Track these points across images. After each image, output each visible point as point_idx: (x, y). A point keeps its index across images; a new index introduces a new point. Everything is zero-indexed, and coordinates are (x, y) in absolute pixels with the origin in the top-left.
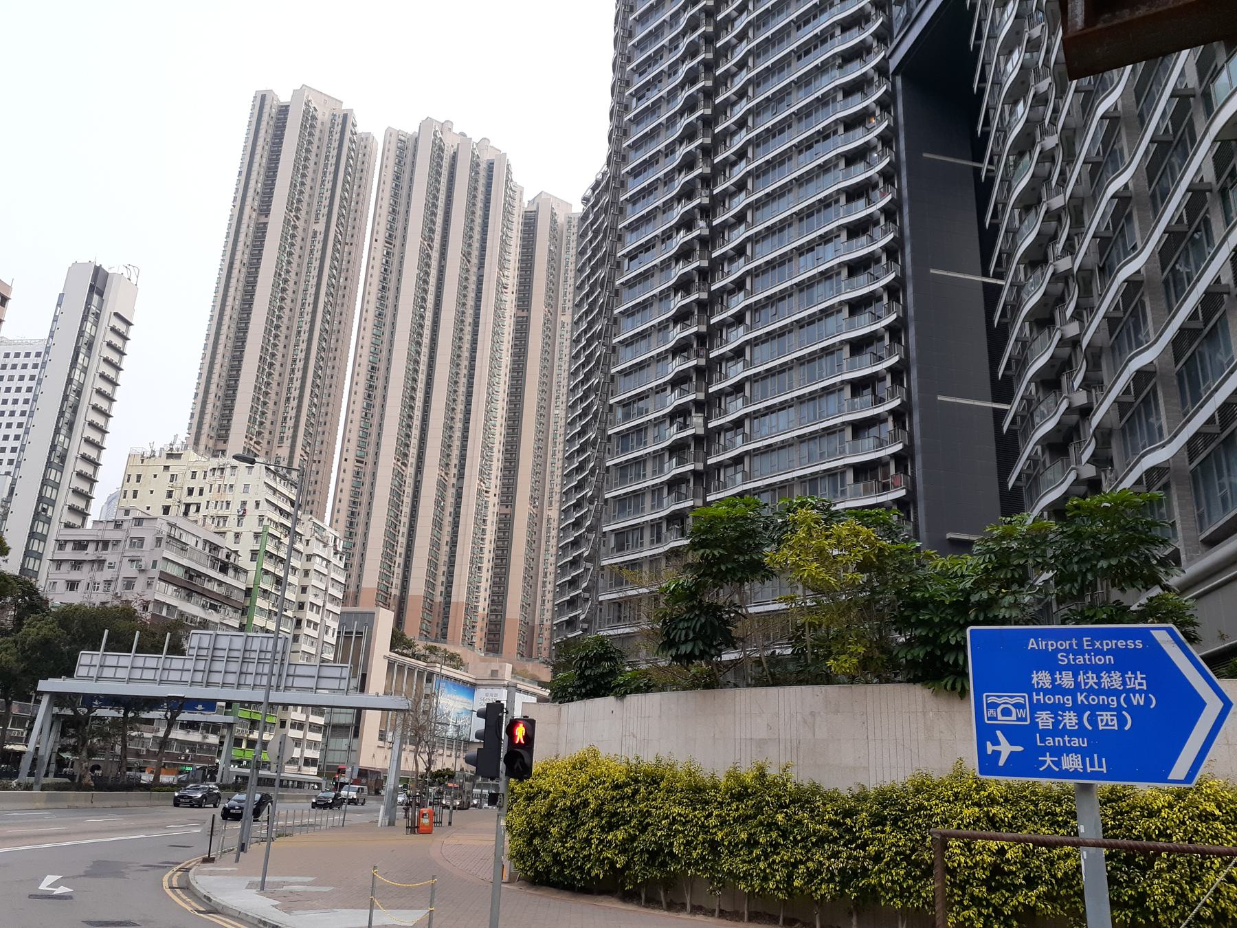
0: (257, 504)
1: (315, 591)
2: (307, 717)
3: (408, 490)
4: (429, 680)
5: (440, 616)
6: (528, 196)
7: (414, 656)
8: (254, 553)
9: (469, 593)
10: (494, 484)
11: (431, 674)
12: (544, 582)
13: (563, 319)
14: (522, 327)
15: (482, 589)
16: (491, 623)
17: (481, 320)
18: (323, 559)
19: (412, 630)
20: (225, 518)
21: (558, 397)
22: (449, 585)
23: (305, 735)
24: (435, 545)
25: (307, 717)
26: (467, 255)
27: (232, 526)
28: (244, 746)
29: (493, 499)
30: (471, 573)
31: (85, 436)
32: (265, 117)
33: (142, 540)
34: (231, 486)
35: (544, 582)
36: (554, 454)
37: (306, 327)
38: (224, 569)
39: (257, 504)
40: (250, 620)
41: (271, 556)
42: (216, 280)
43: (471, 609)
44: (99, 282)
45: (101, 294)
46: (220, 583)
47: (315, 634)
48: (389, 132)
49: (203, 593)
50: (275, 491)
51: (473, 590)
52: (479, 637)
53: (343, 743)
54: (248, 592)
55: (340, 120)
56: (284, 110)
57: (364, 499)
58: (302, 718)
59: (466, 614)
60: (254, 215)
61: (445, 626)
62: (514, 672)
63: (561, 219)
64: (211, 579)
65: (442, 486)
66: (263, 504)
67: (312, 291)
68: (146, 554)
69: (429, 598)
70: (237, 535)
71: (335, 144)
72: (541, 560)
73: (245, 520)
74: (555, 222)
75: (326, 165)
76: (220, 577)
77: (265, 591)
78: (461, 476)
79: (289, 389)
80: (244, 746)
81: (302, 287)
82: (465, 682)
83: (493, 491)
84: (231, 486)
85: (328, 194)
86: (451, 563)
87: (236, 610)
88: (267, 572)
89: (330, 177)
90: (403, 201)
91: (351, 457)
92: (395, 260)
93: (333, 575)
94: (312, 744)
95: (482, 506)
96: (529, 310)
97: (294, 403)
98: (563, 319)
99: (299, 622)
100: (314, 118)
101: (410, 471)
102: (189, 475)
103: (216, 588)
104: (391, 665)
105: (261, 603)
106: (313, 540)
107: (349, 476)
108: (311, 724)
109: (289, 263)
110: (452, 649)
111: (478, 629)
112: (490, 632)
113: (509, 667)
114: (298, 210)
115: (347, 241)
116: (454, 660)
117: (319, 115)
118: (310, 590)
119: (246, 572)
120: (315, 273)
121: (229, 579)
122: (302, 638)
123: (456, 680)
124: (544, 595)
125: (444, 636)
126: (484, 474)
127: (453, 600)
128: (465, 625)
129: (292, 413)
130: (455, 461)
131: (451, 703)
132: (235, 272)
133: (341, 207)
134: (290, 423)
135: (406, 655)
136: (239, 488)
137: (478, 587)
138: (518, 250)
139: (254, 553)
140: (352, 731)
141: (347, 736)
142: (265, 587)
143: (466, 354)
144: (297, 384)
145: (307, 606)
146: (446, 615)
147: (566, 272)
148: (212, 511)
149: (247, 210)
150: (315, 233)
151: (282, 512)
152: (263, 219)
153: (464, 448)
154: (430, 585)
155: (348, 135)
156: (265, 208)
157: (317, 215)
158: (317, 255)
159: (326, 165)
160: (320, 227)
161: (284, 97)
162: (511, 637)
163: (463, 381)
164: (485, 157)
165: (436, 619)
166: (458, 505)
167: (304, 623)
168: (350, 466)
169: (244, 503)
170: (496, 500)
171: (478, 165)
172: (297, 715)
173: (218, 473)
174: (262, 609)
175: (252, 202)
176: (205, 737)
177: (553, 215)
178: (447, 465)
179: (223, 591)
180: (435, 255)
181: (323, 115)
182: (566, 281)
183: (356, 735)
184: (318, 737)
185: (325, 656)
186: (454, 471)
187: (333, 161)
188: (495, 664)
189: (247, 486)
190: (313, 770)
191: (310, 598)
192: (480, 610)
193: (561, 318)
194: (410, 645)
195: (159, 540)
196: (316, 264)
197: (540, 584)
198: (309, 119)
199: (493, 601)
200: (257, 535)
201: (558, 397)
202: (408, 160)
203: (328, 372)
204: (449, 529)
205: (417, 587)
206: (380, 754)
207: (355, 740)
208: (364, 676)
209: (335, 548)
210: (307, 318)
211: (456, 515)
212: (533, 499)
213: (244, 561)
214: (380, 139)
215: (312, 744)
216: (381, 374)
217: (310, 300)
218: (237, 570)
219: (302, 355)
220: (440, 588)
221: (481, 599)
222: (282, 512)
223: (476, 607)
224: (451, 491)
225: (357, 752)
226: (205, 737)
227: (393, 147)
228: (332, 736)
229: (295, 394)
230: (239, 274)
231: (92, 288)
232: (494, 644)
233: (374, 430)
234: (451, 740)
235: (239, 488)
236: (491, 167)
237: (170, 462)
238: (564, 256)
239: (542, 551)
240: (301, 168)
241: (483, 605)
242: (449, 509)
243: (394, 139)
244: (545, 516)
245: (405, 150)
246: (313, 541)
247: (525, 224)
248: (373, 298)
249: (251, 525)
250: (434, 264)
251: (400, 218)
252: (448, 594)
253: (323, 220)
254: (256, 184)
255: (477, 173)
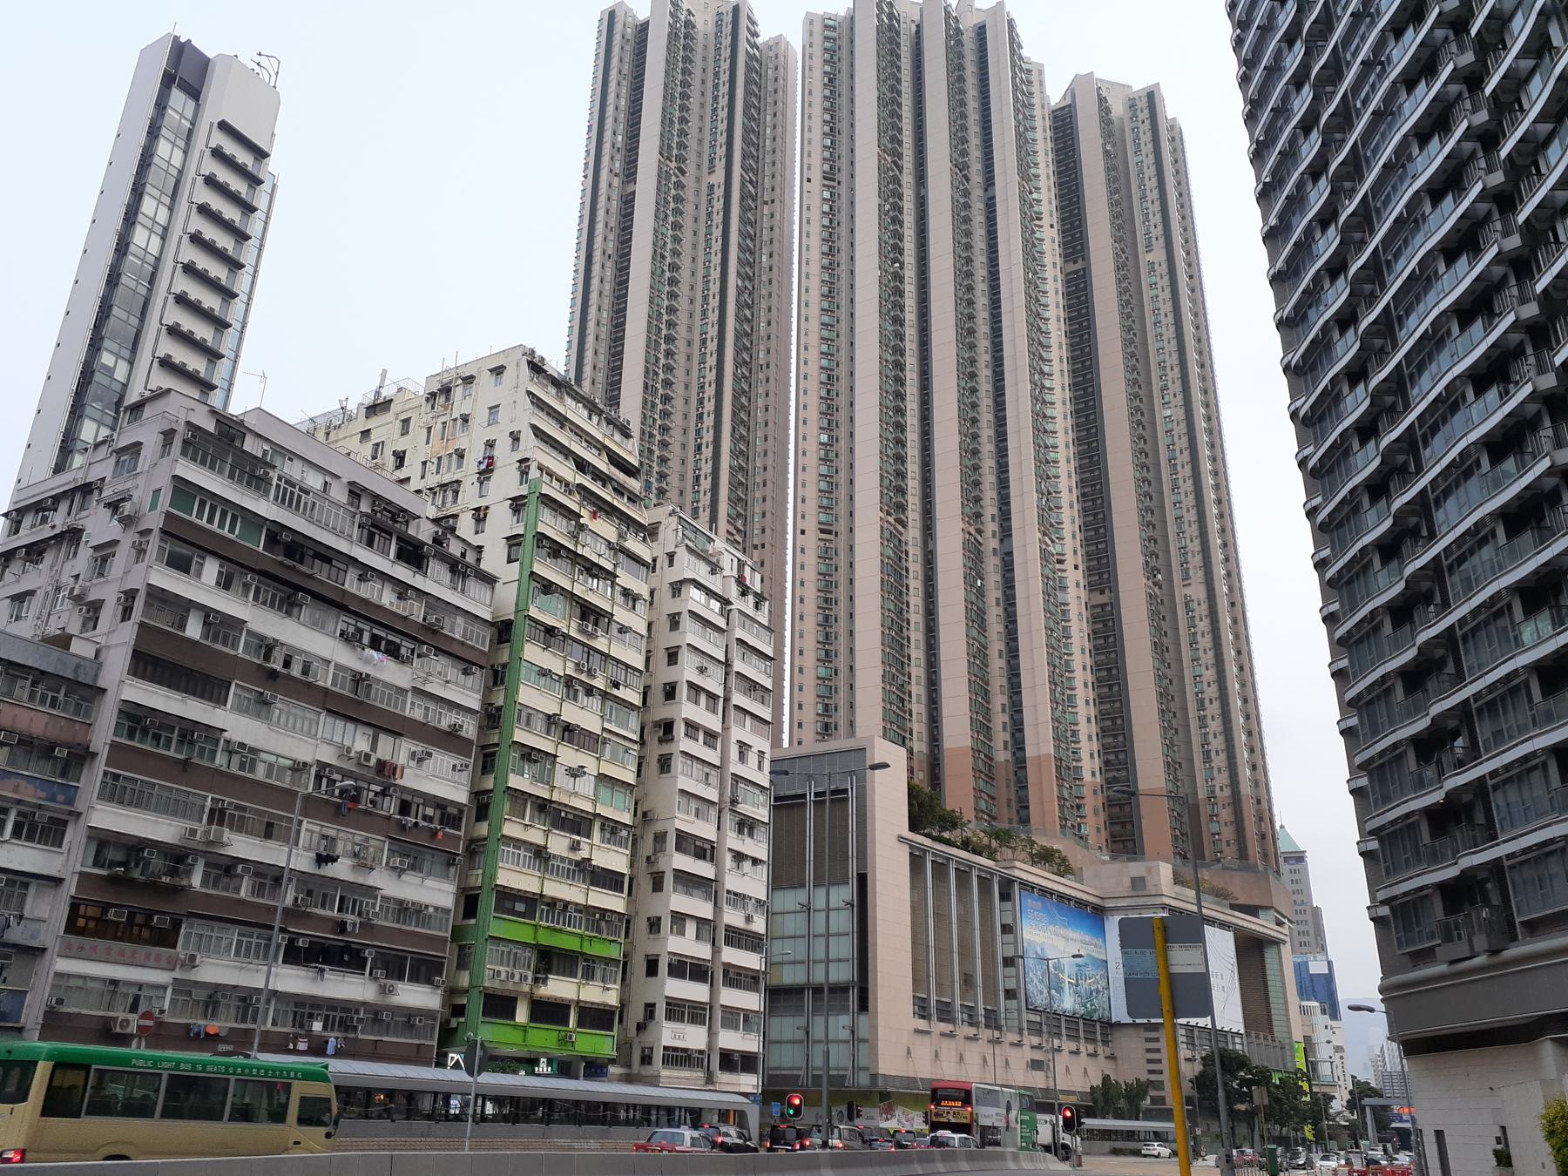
0: (515, 437)
1: (696, 660)
2: (716, 951)
3: (915, 566)
4: (1006, 896)
5: (1007, 780)
6: (1055, 93)
7: (965, 845)
8: (514, 541)
9: (1057, 738)
10: (1071, 544)
11: (1007, 885)
12: (1202, 719)
13: (1150, 257)
14: (1078, 291)
15: (1083, 737)
16: (1110, 803)
17: (1010, 412)
18: (710, 593)
19: (959, 794)
20: (454, 487)
21: (1164, 388)
22: (1017, 727)
23: (713, 993)
24: (978, 656)
25: (716, 951)
26: (960, 168)
27: (469, 497)
28: (522, 1015)
29: (1074, 576)
30: (1054, 701)
31: (161, 353)
32: (617, 39)
33: (136, 447)
34: (465, 419)
35: (1202, 719)
36: (1175, 488)
37: (713, 332)
38: (413, 554)
39: (515, 437)
40: (512, 694)
41: (556, 551)
42: (570, 289)
43: (1066, 771)
44: (184, 71)
45: (195, 93)
46: (403, 589)
47: (713, 756)
48: (810, 20)
49: (338, 604)
50: (562, 421)
51: (1065, 736)
52: (1093, 823)
53: (840, 1025)
54: (503, 631)
55: (730, 18)
56: (643, 29)
57: (841, 593)
58: (703, 951)
59: (1060, 778)
60: (616, 182)
61: (1024, 805)
62: (1178, 880)
63: (1118, 109)
64: (366, 572)
65: (974, 552)
66: (528, 439)
67: (715, 274)
68: (141, 480)
69: (985, 767)
70: (480, 515)
71: (726, 53)
72: (1188, 680)
73: (495, 476)
74: (1108, 111)
75: (716, 86)
76: (402, 572)
77: (550, 631)
78: (1006, 533)
79: (698, 432)
80: (522, 1015)
81: (701, 272)
82: (1081, 904)
83: (1070, 560)
84: (465, 419)
85: (723, 126)
86: (1014, 688)
87: (466, 662)
88: (548, 587)
89: (723, 101)
90: (844, 113)
91: (811, 525)
92: (843, 202)
93: (739, 633)
94: (733, 1017)
95: (1053, 587)
96: (1085, 258)
97: (707, 452)
98: (1150, 257)
99: (668, 727)
100: (689, 24)
101: (913, 533)
102: (398, 425)
103: (388, 598)
104: (916, 861)
105: (533, 653)
106: (682, 554)
107: (811, 559)
108: (728, 968)
109: (677, 240)
110: (1042, 841)
111: (1088, 810)
112: (1112, 821)
113: (1165, 871)
114: (681, 159)
115: (756, 195)
116: (1045, 857)
117: (700, 26)
118: (685, 656)
119: (489, 580)
120: (717, 246)
121: (435, 581)
122: (678, 763)
123: (1062, 897)
124: (1205, 743)
125: (1025, 821)
126: (1048, 527)
127: (1030, 752)
128: (1061, 798)
129: (707, 468)
130: (990, 509)
131: (1060, 943)
132: (596, 268)
133: (745, 140)
134: (706, 484)
135: (948, 842)
136: (480, 417)
137: (1074, 733)
138: (1050, 145)
139: (514, 541)
140: (853, 996)
141: (844, 1009)
142: (550, 621)
143: (983, 328)
144: (709, 421)
145: (683, 692)
146: (1022, 785)
147: (1142, 184)
148: (433, 480)
149: (604, 174)
150: (711, 187)
151: (582, 466)
152: (629, 189)
153: (1003, 484)
154: (982, 727)
155: (743, 46)
156: (630, 174)
157: (711, 161)
158: (718, 219)
159: (716, 86)
160: (718, 177)
161: (642, 12)
162: (1156, 823)
163: (984, 373)
164: (968, 24)
165: (1005, 792)
166: (1008, 584)
167: (680, 729)
168: (812, 540)
169: (490, 444)
170: (1079, 575)
171: (959, 32)
172: (689, 945)
173: (441, 400)
174: (544, 673)
175: (612, 163)
176: (385, 991)
177: (1102, 100)
178: (978, 516)
179: (416, 611)
180: (907, 179)
181: (704, 23)
182: (1143, 197)
183: (864, 1005)
184: (751, 1001)
185: (745, 808)
186: (991, 527)
187: (725, 77)
188: (1136, 868)
189: (494, 409)
190: (749, 1082)
191: (687, 671)
192: (1086, 775)
193: (1145, 258)
194: (951, 821)
195: (168, 435)
196: (717, 232)
197: (1194, 724)
198: (682, 34)
199: (1107, 763)
200: (517, 504)
201: (1164, 388)
202: (844, 53)
203: (760, 403)
204: (1001, 628)
205: (957, 732)
206: (923, 1049)
207: (863, 1020)
208: (862, 879)
209: (740, 580)
210: (713, 317)
211: (1009, 602)
212: (1151, 572)
213: (495, 559)
214: (796, 42)
215: (733, 1017)
216: (842, 386)
217: (715, 288)
218: (463, 570)
219: (711, 376)
220: (1001, 737)
221: (1085, 755)
222: (582, 466)
223: (1078, 769)
224: (992, 564)
225: (871, 1042)
226: (385, 991)
227: (818, 39)
228: (816, 1011)
229: (708, 437)
230: (603, 272)
231: (168, 80)
232: (1124, 838)
233: (842, 478)
234: (1072, 1019)
235: (480, 417)
236: (981, 31)
237: (371, 424)
238: (1132, 160)
239: (1186, 662)
240: (677, 94)
241: (1089, 766)
242: (994, 593)
243: (818, 28)
244: (1179, 600)
245: (834, 40)
246: (683, 556)
247: (1055, 129)
248: (815, 269)
249: (506, 483)
250: (908, 193)
251: (843, 138)
252: (1018, 744)
253: (720, 166)
254: (615, 137)
255: (959, 43)
